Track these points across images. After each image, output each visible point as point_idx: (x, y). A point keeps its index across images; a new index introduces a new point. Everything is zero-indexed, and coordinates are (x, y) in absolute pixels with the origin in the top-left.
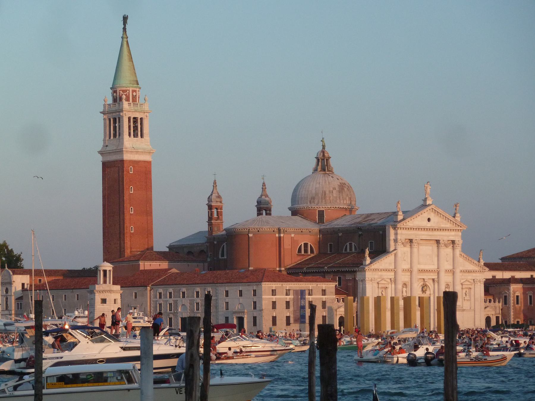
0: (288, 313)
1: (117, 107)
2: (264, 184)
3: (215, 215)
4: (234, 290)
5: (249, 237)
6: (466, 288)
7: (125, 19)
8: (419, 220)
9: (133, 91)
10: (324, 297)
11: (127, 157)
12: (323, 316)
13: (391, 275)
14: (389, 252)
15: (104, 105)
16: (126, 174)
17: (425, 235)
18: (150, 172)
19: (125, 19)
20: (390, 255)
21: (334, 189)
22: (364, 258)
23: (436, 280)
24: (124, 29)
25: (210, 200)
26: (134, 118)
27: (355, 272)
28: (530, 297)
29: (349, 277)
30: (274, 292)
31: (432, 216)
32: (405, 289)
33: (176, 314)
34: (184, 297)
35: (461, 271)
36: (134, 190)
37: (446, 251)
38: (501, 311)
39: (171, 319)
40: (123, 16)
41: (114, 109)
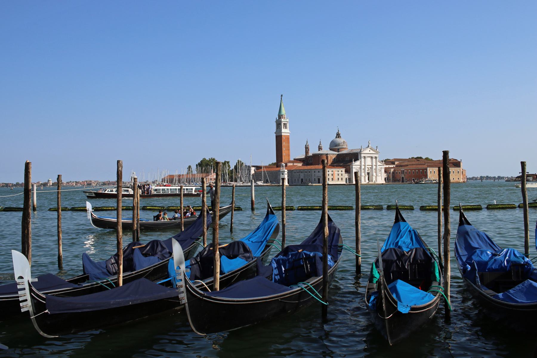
2: (320, 142)
3: (307, 150)
5: (319, 156)
7: (282, 96)
8: (367, 151)
11: (283, 134)
14: (359, 160)
15: (276, 120)
19: (282, 96)
20: (359, 161)
22: (352, 161)
24: (281, 99)
25: (306, 145)
27: (350, 166)
29: (348, 167)
30: (329, 171)
33: (300, 178)
34: (302, 173)
37: (374, 160)
39: (298, 179)
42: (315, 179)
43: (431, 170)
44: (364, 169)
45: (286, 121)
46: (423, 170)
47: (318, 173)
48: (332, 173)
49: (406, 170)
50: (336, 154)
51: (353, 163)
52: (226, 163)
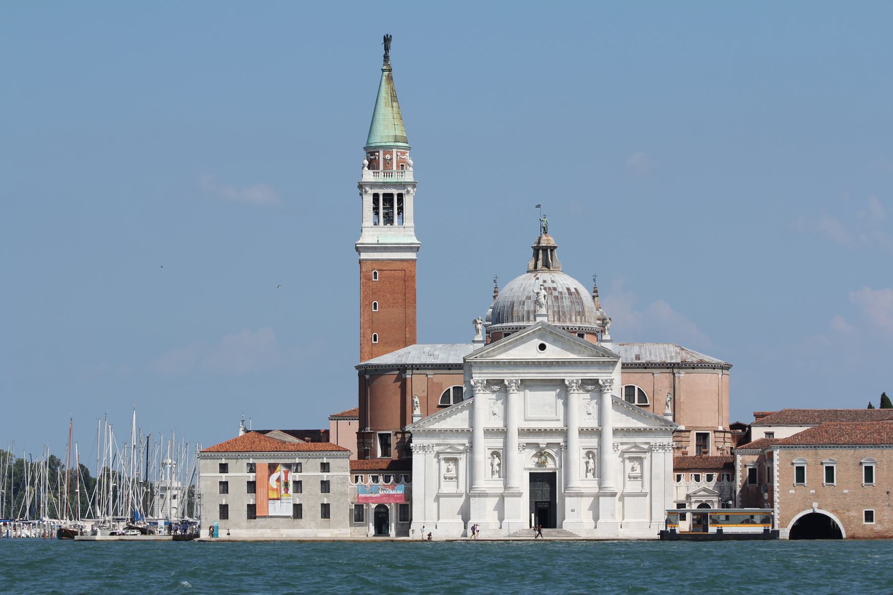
0: (252, 500)
6: (630, 458)
7: (387, 40)
9: (384, 154)
10: (325, 476)
12: (323, 505)
16: (366, 282)
18: (413, 278)
19: (387, 40)
21: (529, 298)
23: (562, 444)
24: (386, 58)
26: (384, 195)
30: (224, 468)
32: (497, 461)
35: (617, 430)
36: (381, 307)
38: (733, 495)
40: (384, 36)
43: (798, 462)
44: (501, 455)
48: (252, 477)
51: (415, 419)
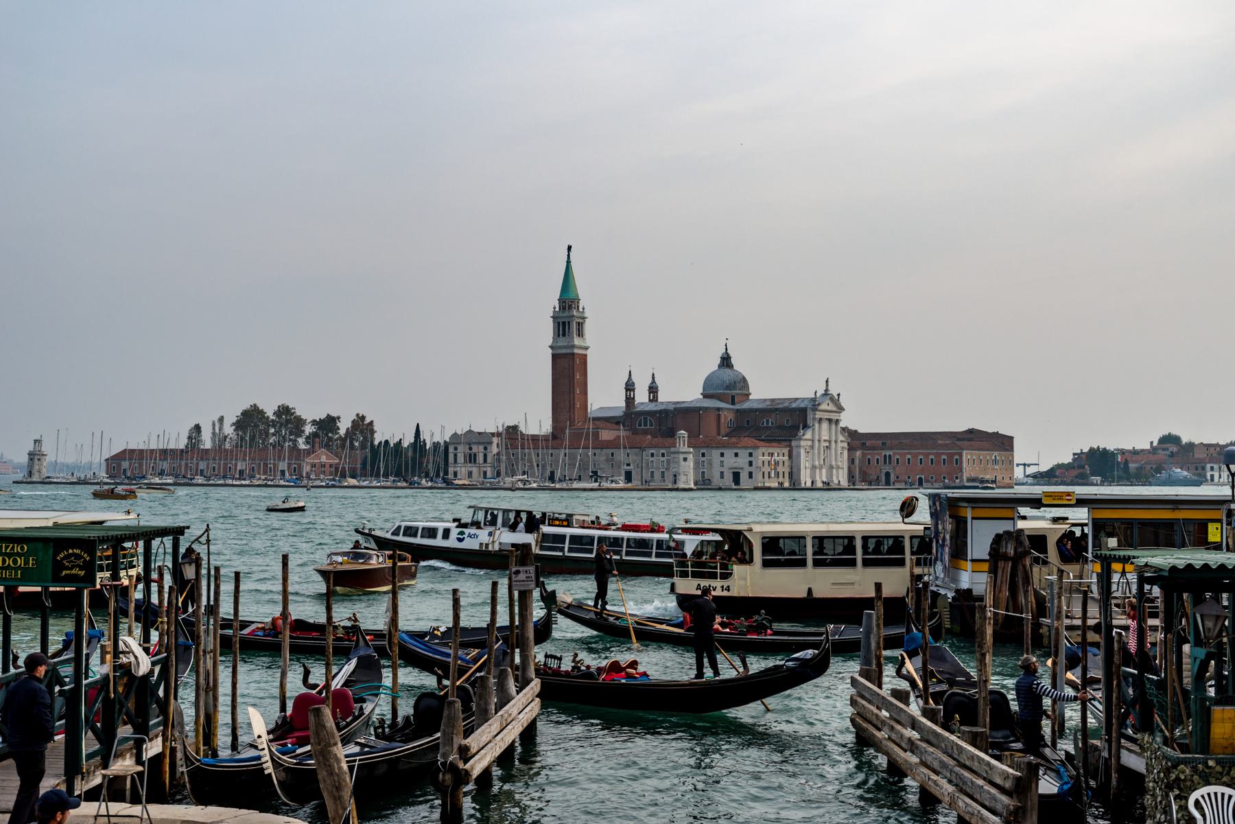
1: (566, 314)
2: (653, 375)
4: (729, 453)
11: (576, 351)
13: (810, 443)
15: (554, 312)
17: (826, 416)
19: (569, 248)
22: (798, 429)
24: (569, 256)
25: (627, 384)
27: (790, 441)
28: (869, 459)
31: (829, 402)
37: (834, 426)
39: (663, 472)
41: (564, 315)
42: (722, 473)
45: (580, 315)
46: (951, 456)
47: (734, 459)
49: (899, 454)
50: (733, 409)
52: (329, 424)
